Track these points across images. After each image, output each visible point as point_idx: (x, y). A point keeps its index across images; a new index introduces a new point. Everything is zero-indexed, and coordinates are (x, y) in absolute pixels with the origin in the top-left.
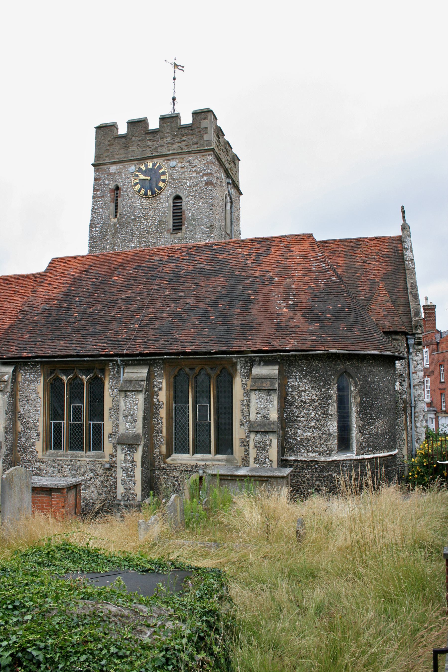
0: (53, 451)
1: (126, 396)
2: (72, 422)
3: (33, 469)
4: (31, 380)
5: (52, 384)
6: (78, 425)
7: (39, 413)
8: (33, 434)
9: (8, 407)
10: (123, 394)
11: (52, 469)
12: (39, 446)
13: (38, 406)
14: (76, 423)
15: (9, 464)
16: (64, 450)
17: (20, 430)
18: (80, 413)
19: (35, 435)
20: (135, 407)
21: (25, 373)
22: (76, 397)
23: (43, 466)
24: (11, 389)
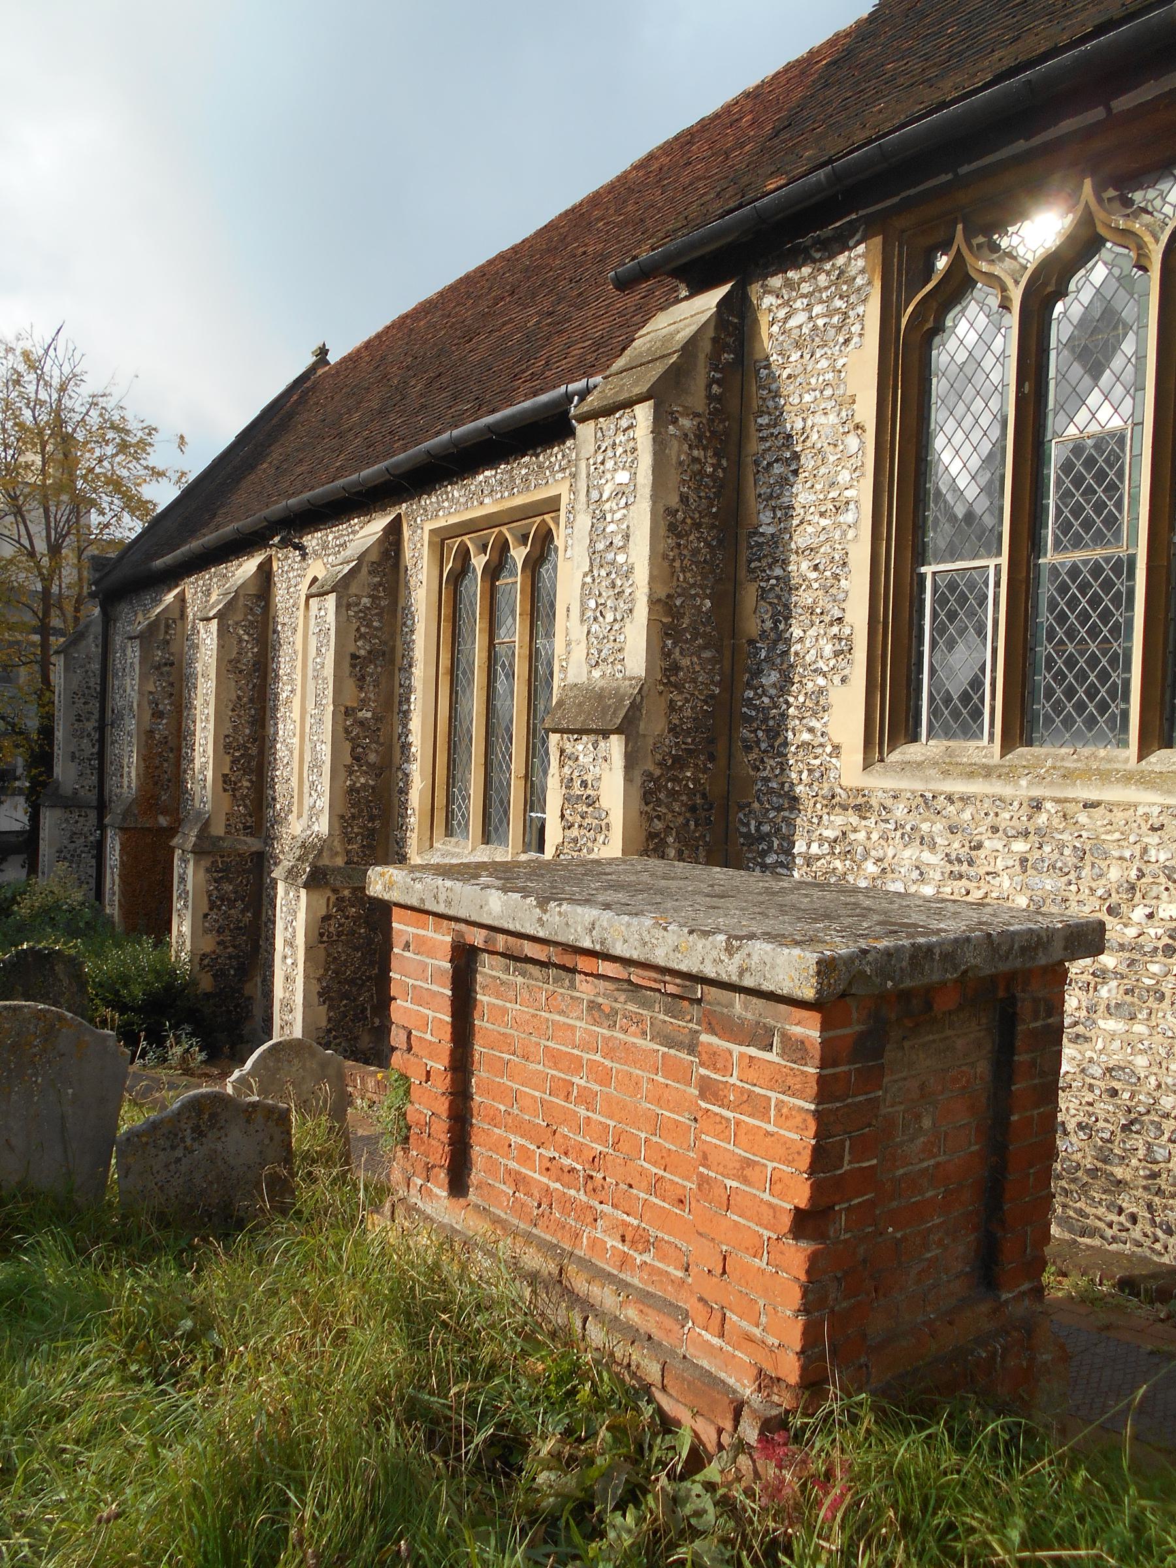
0: (925, 749)
6: (1097, 570)
7: (849, 517)
9: (684, 499)
11: (910, 854)
13: (844, 477)
14: (1077, 556)
15: (693, 809)
19: (828, 650)
21: (787, 303)
23: (865, 833)
24: (710, 397)
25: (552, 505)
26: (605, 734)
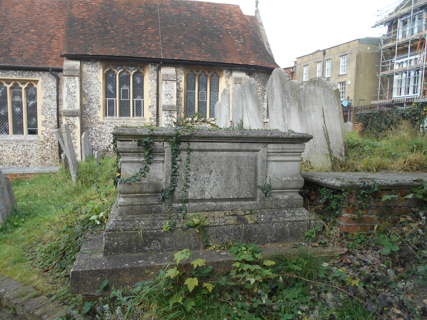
0: (108, 117)
1: (166, 83)
2: (121, 99)
3: (96, 128)
4: (93, 71)
5: (106, 75)
8: (95, 106)
10: (164, 82)
11: (110, 128)
12: (100, 113)
16: (116, 116)
17: (85, 103)
18: (127, 94)
19: (97, 107)
20: (172, 90)
22: (124, 84)
23: (103, 126)
25: (36, 82)
26: (75, 116)
